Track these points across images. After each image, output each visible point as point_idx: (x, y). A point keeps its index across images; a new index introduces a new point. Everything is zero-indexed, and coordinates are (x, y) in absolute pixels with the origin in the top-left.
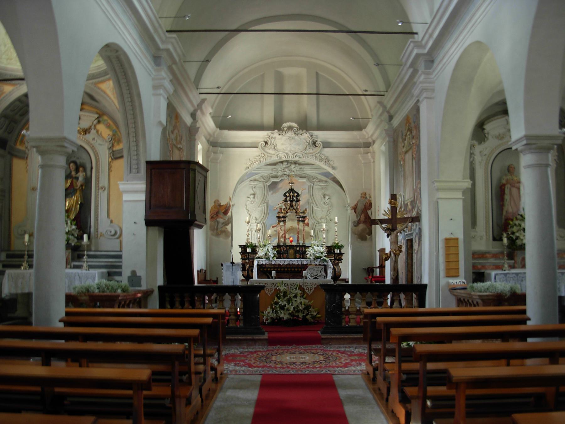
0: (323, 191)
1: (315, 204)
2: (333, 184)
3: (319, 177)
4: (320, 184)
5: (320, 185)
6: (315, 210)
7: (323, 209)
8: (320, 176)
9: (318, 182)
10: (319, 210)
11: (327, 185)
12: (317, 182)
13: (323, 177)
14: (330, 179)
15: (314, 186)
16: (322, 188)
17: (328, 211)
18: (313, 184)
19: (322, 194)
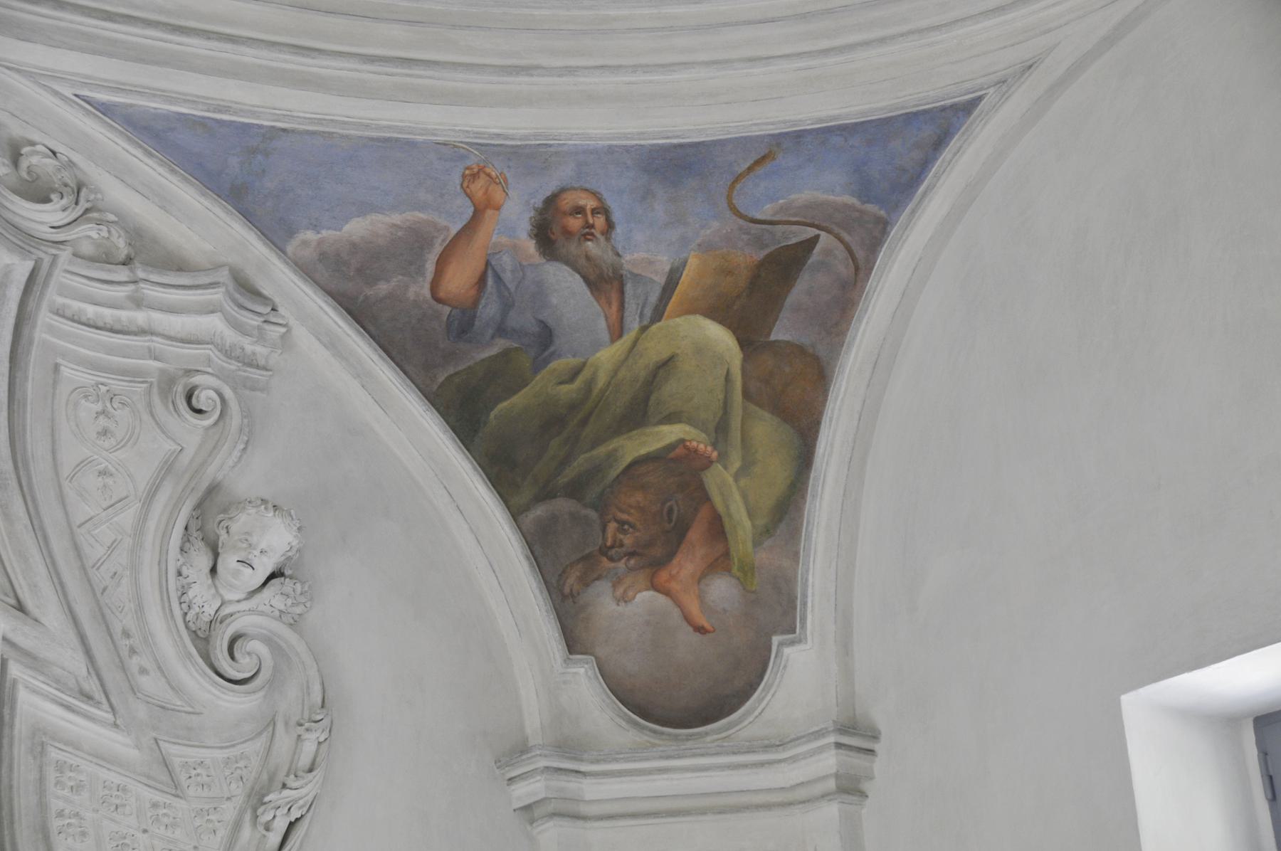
0: (190, 430)
1: (52, 616)
2: (332, 345)
3: (116, 194)
4: (138, 302)
5: (140, 317)
6: (42, 739)
7: (177, 752)
8: (151, 169)
9: (105, 258)
10: (103, 758)
11: (249, 346)
12: (92, 259)
13: (188, 195)
14: (305, 270)
15: (44, 317)
16: (167, 383)
17: (257, 800)
18: (22, 269)
19: (168, 467)
